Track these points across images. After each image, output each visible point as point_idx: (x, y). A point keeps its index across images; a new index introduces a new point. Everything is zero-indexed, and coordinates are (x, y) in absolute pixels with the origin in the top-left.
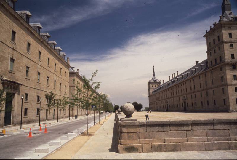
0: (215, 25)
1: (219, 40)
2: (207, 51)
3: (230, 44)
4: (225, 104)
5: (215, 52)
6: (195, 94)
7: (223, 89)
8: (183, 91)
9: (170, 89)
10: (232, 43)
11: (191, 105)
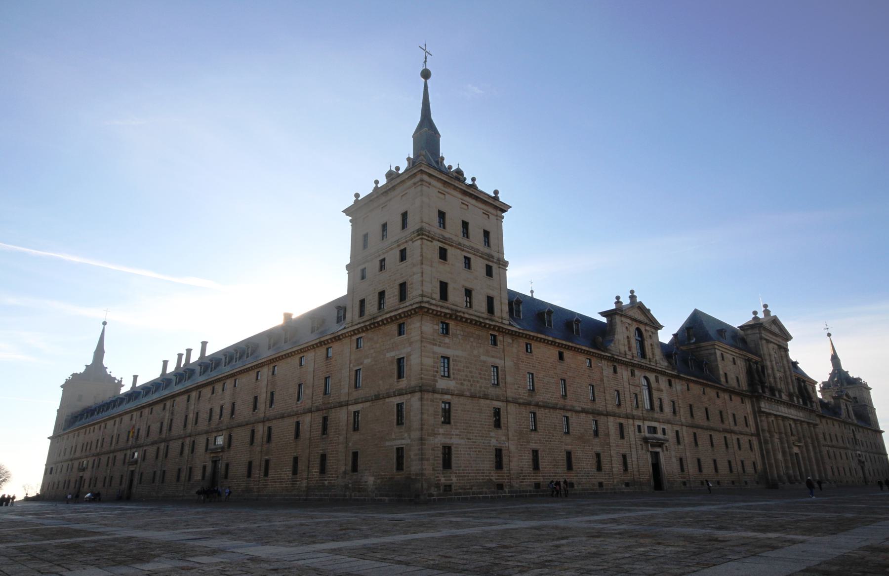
0: (390, 175)
1: (404, 225)
2: (348, 261)
3: (441, 245)
6: (270, 428)
7: (400, 406)
8: (216, 416)
9: (162, 406)
10: (446, 247)
11: (243, 470)
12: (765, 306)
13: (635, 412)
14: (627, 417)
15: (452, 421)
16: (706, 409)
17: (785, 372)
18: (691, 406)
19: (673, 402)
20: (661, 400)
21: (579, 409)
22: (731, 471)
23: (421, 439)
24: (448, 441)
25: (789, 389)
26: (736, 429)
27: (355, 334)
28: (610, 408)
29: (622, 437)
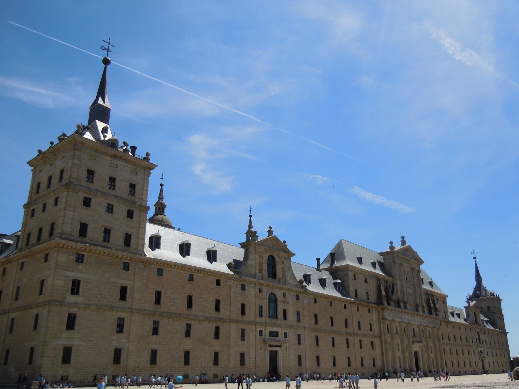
1: (61, 179)
2: (26, 202)
4: (30, 362)
5: (44, 210)
7: (37, 316)
12: (403, 237)
13: (258, 320)
14: (250, 323)
15: (76, 328)
16: (332, 318)
17: (415, 288)
18: (316, 316)
19: (298, 313)
20: (285, 312)
21: (203, 318)
22: (349, 365)
23: (44, 341)
24: (68, 343)
26: (360, 332)
27: (20, 259)
28: (233, 317)
29: (243, 338)
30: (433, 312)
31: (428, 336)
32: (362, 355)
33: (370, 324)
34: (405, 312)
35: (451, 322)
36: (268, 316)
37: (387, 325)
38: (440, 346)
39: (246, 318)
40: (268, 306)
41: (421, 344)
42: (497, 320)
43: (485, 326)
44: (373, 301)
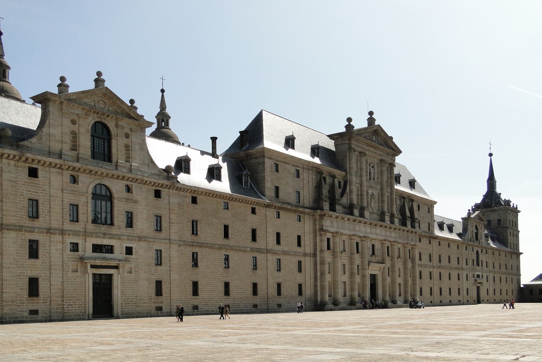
19: (159, 219)
25: (382, 207)
30: (409, 223)
31: (396, 255)
32: (279, 280)
33: (299, 237)
34: (360, 222)
35: (437, 238)
36: (90, 220)
37: (328, 240)
38: (413, 267)
39: (41, 222)
40: (90, 205)
41: (382, 265)
42: (509, 237)
43: (489, 244)
44: (307, 205)
